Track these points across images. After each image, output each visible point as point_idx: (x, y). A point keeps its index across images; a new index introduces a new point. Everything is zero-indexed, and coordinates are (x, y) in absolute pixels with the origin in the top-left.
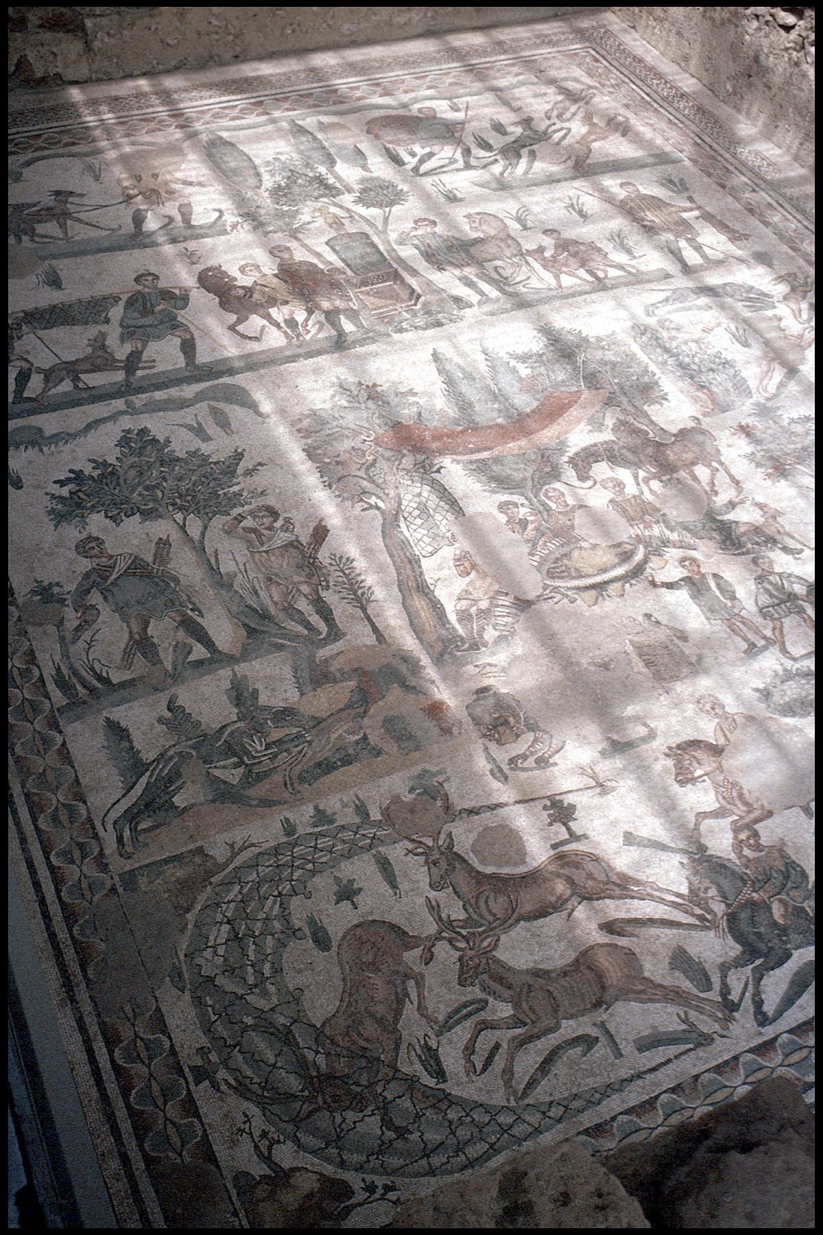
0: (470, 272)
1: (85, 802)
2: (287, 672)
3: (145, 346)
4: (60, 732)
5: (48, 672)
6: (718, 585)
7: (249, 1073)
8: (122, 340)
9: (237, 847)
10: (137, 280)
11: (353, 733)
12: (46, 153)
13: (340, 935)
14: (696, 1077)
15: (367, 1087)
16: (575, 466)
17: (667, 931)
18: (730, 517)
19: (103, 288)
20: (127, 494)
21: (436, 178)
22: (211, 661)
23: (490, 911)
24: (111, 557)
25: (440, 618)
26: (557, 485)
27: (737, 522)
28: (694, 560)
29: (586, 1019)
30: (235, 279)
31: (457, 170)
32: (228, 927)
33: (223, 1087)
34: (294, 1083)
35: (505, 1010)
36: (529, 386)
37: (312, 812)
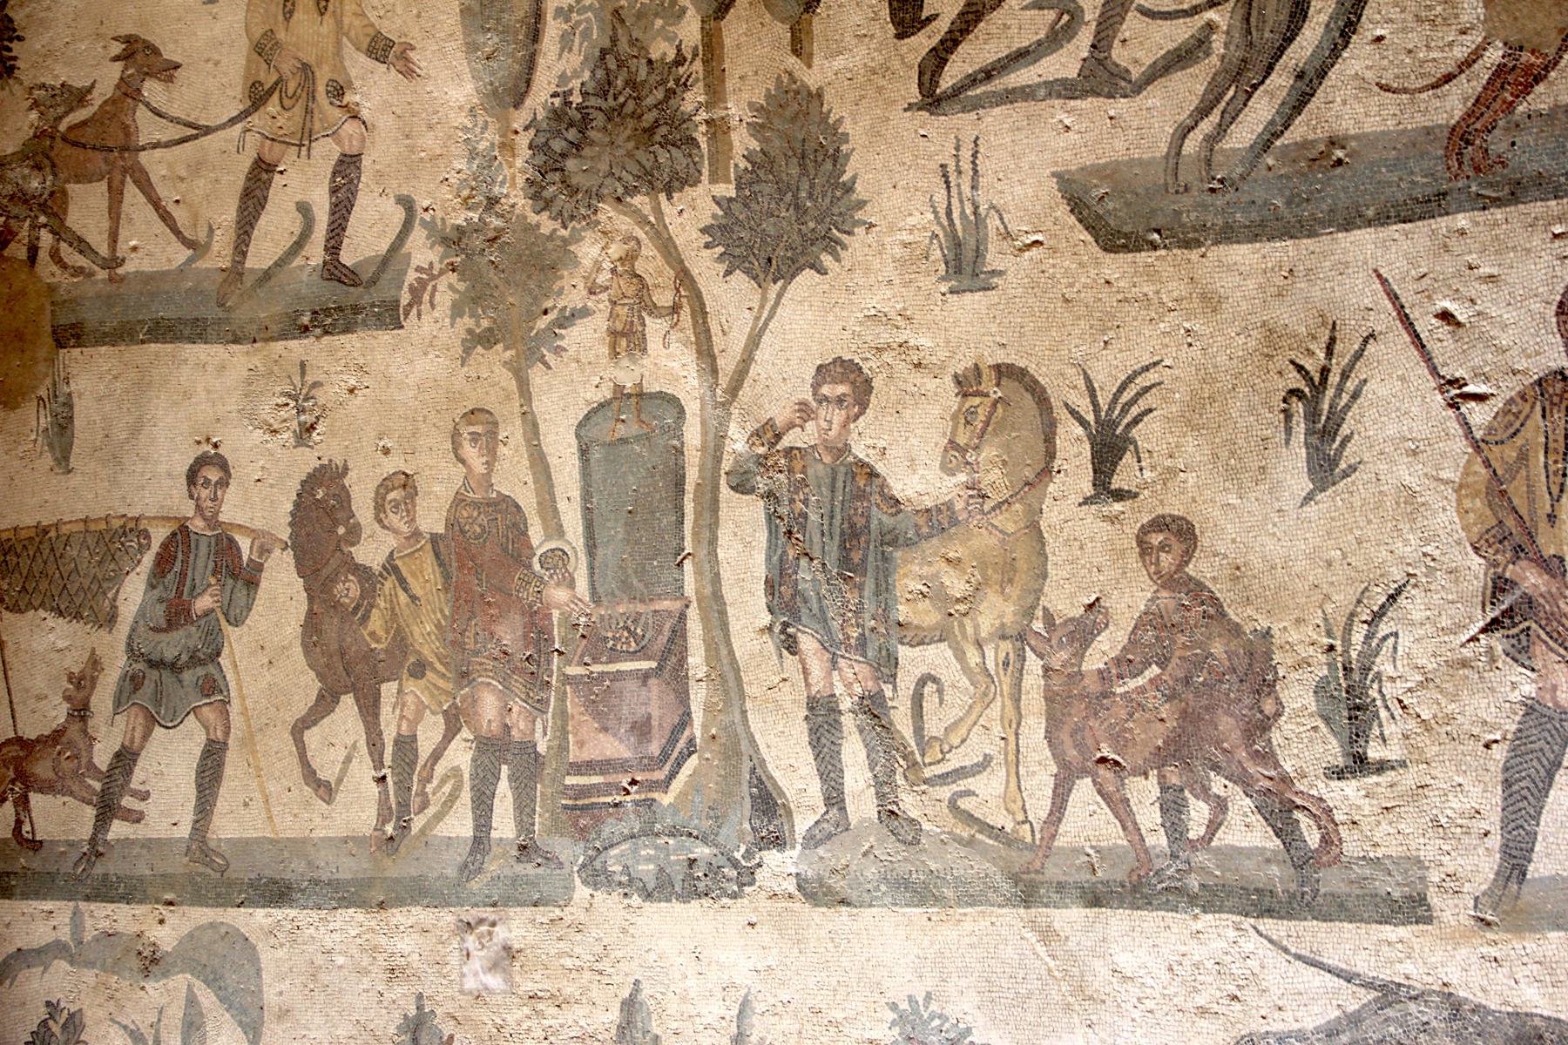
3: (146, 736)
8: (118, 703)
10: (192, 476)
30: (354, 533)
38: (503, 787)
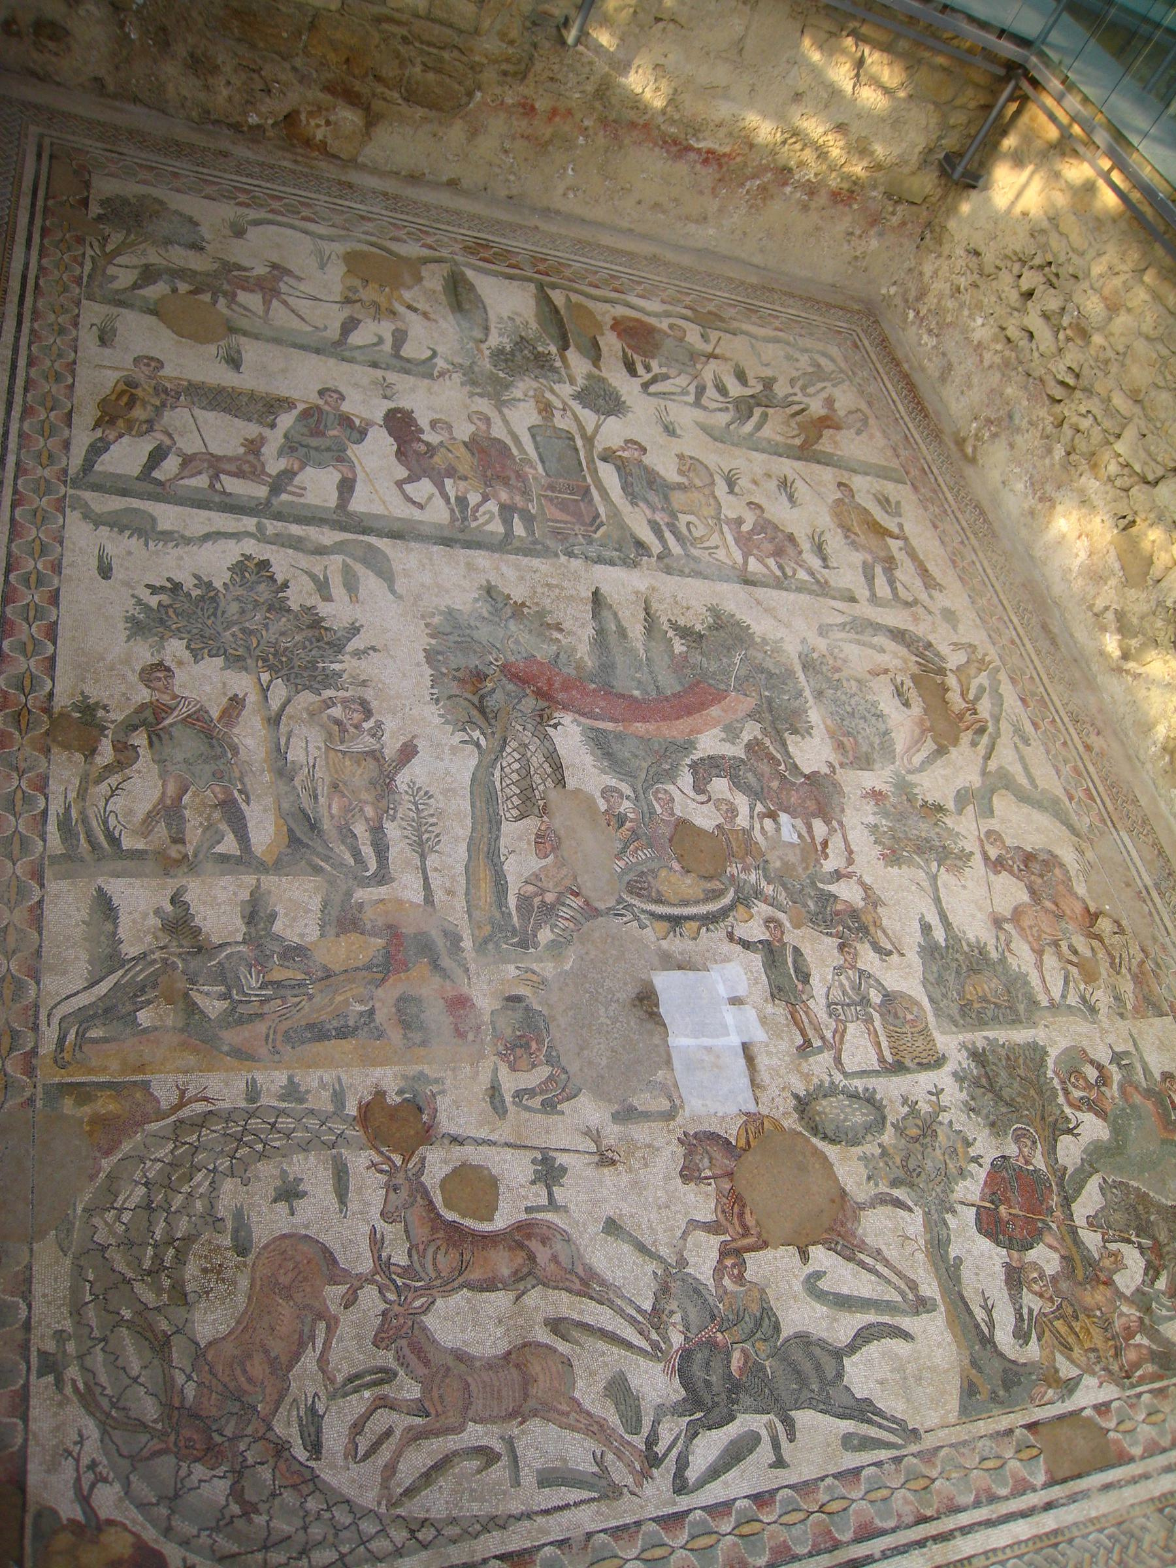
0: (661, 518)
1: (38, 983)
2: (315, 904)
3: (302, 468)
4: (42, 886)
5: (56, 808)
6: (795, 962)
7: (103, 1379)
8: (280, 453)
9: (188, 1096)
10: (321, 393)
11: (361, 1002)
12: (279, 218)
13: (264, 1242)
14: (589, 1535)
15: (229, 1439)
16: (695, 774)
17: (615, 1350)
18: (833, 888)
19: (282, 389)
20: (220, 629)
21: (663, 403)
22: (239, 861)
23: (435, 1264)
24: (175, 697)
25: (499, 898)
26: (670, 788)
27: (836, 897)
28: (779, 924)
29: (495, 1429)
30: (422, 431)
31: (686, 403)
32: (141, 1190)
33: (68, 1390)
34: (150, 1410)
35: (410, 1390)
36: (679, 665)
37: (284, 1082)
38: (517, 521)
